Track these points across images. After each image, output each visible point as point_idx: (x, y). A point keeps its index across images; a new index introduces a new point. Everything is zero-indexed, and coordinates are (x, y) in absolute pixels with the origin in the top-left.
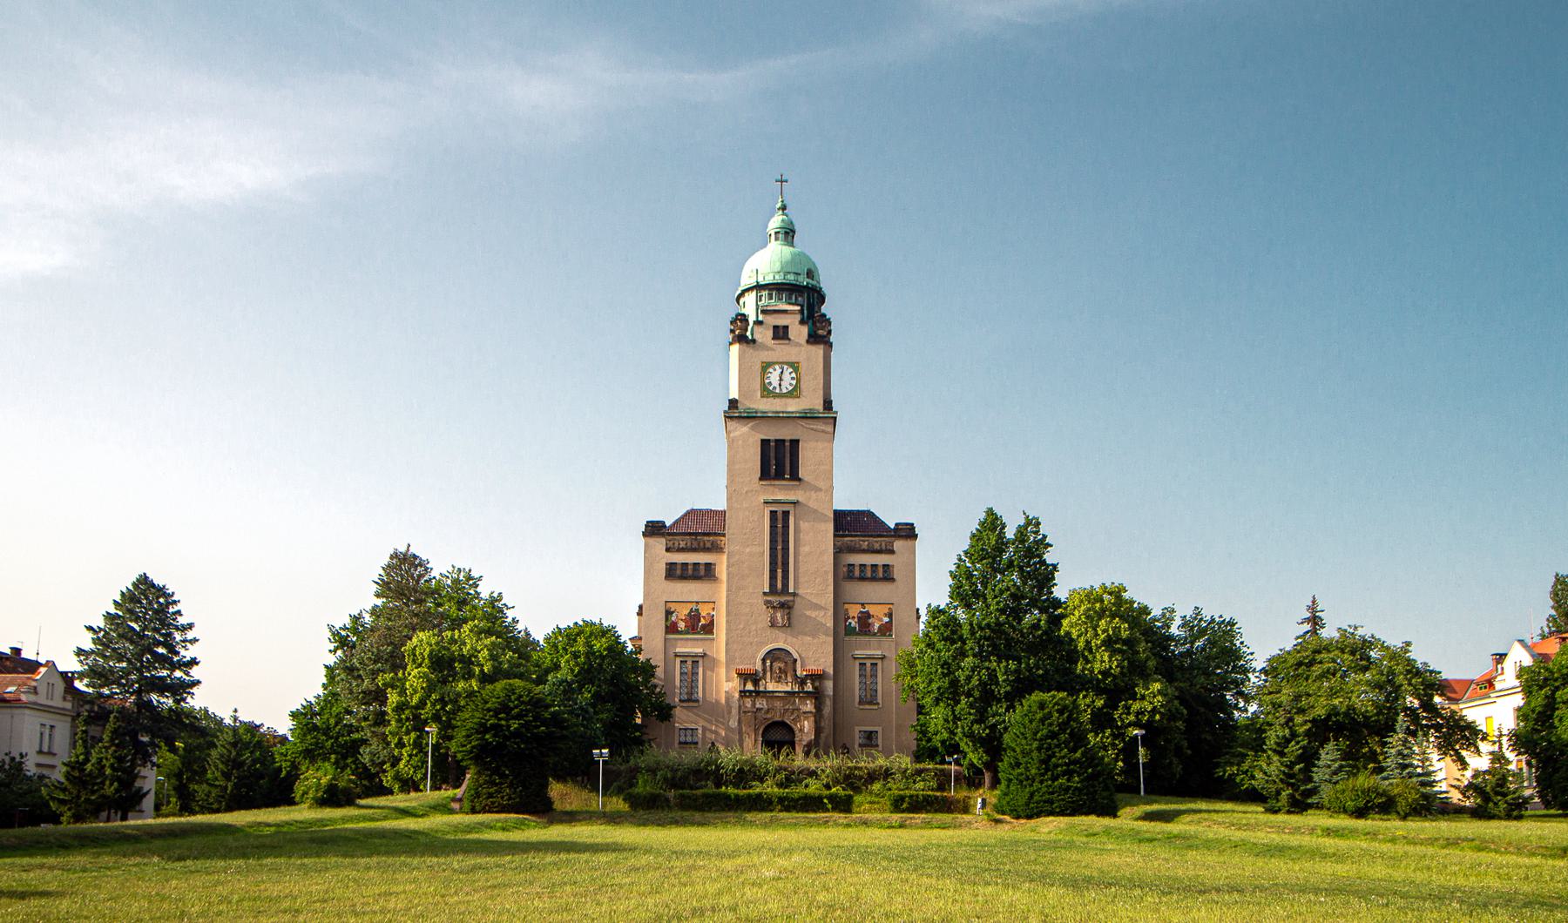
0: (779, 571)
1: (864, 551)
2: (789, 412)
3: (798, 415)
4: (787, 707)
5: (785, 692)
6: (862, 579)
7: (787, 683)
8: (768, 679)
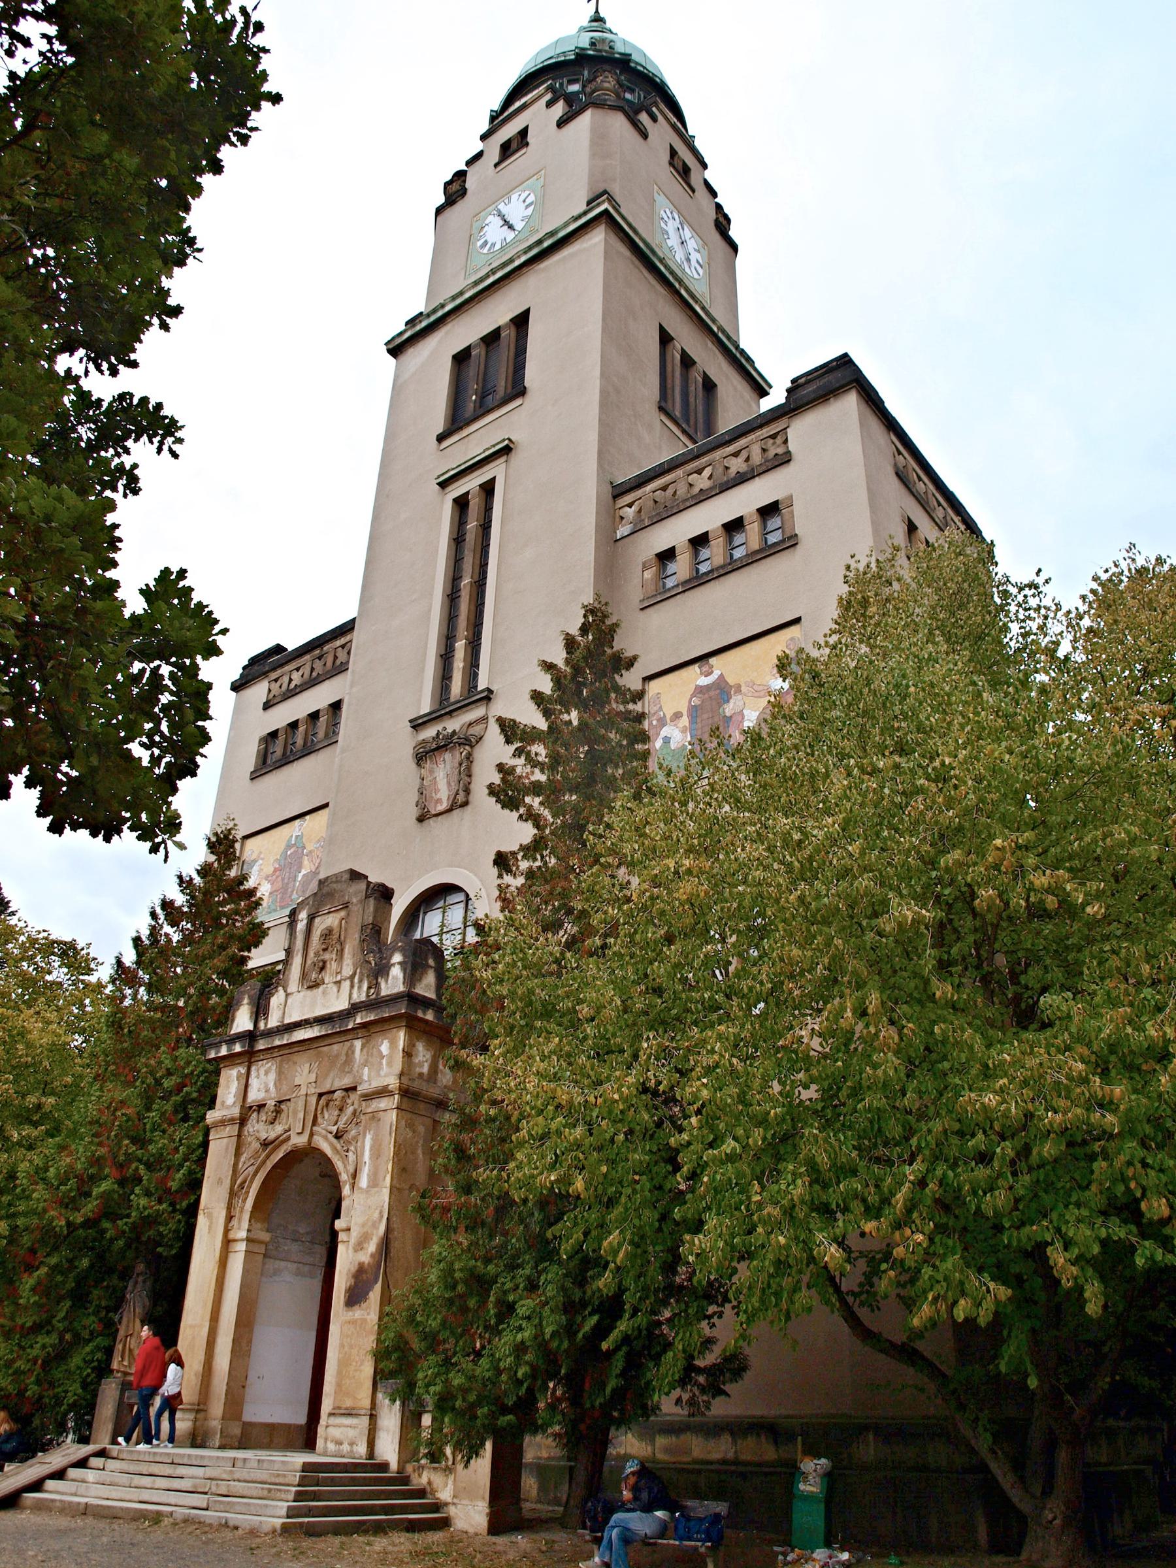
0: (460, 646)
1: (703, 497)
2: (504, 265)
3: (523, 259)
4: (327, 1087)
5: (321, 1020)
6: (697, 581)
7: (338, 983)
8: (293, 985)
